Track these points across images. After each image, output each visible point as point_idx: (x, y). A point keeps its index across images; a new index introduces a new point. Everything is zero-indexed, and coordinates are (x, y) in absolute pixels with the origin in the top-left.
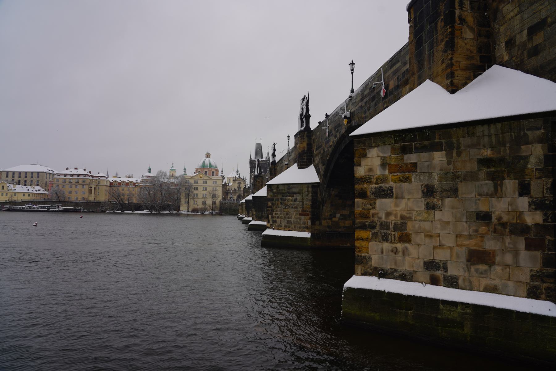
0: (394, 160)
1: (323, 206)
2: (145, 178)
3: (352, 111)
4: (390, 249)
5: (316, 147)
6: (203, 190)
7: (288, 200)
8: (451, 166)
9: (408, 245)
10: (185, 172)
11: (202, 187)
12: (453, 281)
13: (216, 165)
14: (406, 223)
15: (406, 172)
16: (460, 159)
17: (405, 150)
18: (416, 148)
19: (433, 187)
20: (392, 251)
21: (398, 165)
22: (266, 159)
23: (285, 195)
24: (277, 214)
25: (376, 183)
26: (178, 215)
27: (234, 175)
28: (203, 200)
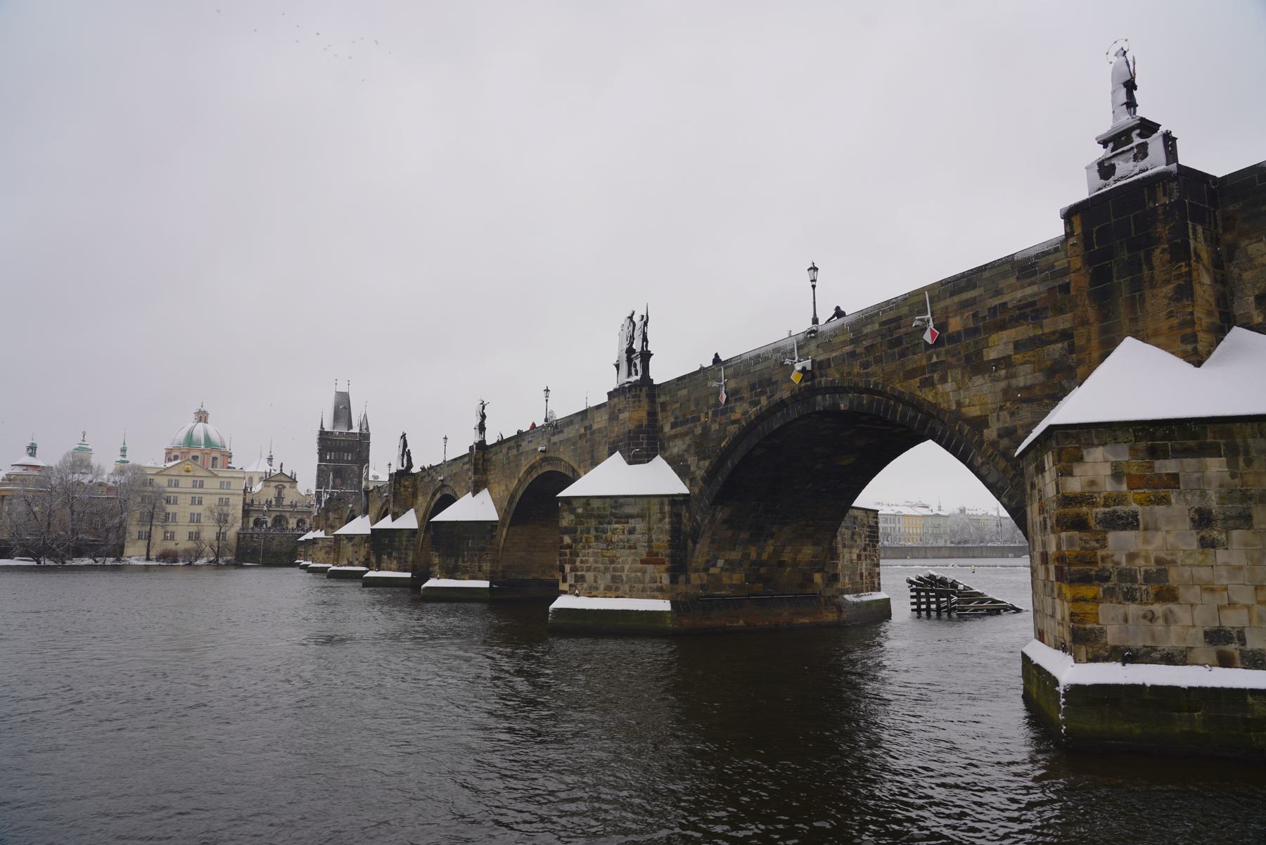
0: (1136, 468)
1: (695, 543)
2: (18, 470)
3: (818, 359)
4: (1141, 613)
5: (672, 420)
6: (193, 503)
7: (614, 531)
8: (1237, 480)
10: (124, 456)
11: (189, 497)
12: (1256, 658)
13: (222, 441)
14: (1166, 571)
15: (1160, 488)
16: (1250, 470)
17: (1154, 453)
18: (1174, 450)
19: (1210, 512)
20: (1145, 617)
21: (1145, 476)
22: (361, 430)
23: (607, 520)
24: (587, 561)
25: (1105, 505)
26: (115, 568)
27: (264, 467)
28: (194, 529)
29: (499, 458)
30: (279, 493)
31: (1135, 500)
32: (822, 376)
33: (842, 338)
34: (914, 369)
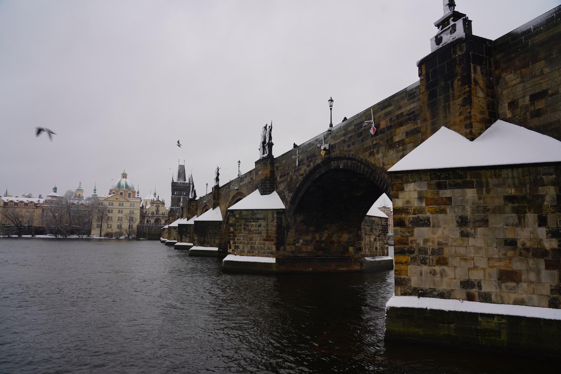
0: (430, 194)
1: (288, 232)
2: (49, 198)
3: (331, 144)
4: (429, 271)
5: (280, 174)
7: (252, 226)
8: (481, 201)
9: (445, 267)
10: (95, 193)
11: (117, 210)
13: (133, 186)
14: (442, 248)
15: (442, 205)
16: (489, 196)
17: (440, 186)
18: (450, 185)
19: (467, 218)
20: (431, 273)
21: (434, 198)
22: (189, 181)
23: (249, 221)
24: (240, 239)
25: (414, 214)
26: (88, 240)
27: (152, 197)
28: (119, 224)
29: (223, 193)
30: (158, 209)
31: (429, 211)
32: (333, 152)
33: (340, 133)
34: (367, 147)
